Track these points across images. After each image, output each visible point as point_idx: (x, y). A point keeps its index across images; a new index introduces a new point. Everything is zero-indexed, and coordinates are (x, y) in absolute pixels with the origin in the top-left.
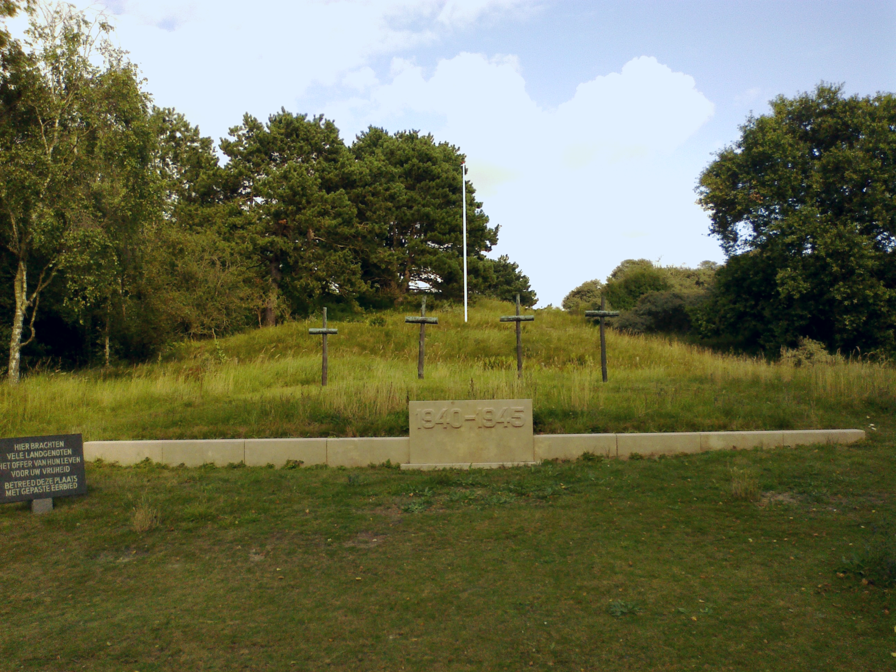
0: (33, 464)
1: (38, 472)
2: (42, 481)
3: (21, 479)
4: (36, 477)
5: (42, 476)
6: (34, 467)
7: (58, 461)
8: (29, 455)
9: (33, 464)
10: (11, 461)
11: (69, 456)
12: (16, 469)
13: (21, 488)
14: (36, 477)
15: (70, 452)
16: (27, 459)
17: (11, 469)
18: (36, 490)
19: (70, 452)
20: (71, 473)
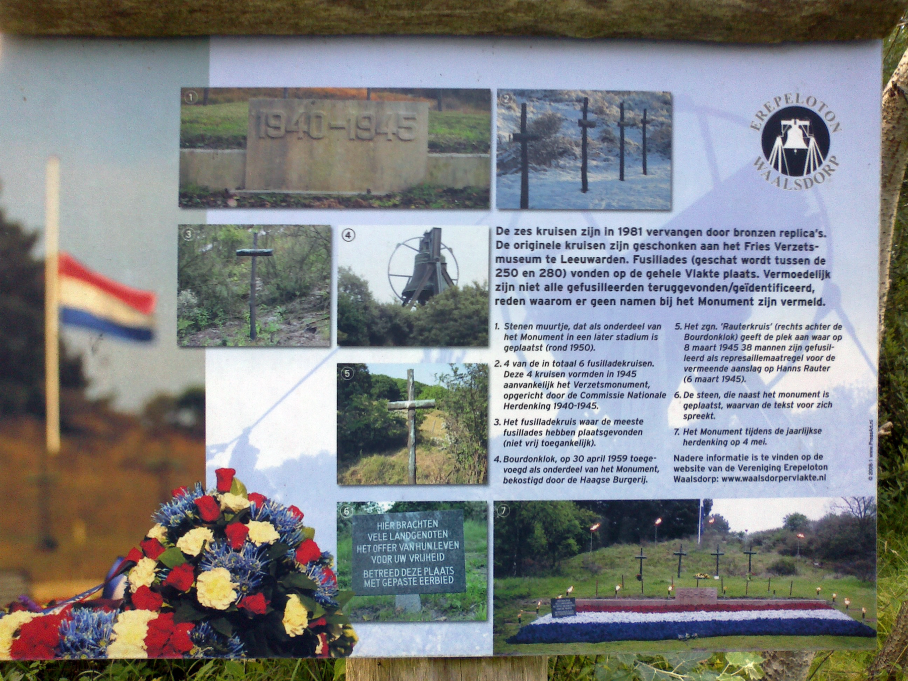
0: (398, 548)
1: (403, 559)
2: (407, 571)
3: (383, 566)
4: (400, 565)
5: (408, 564)
6: (399, 552)
7: (429, 546)
8: (393, 537)
9: (398, 548)
10: (372, 543)
11: (445, 540)
12: (378, 554)
13: (382, 578)
14: (400, 565)
15: (446, 534)
16: (392, 542)
17: (373, 554)
18: (400, 583)
19: (446, 534)
20: (446, 563)
